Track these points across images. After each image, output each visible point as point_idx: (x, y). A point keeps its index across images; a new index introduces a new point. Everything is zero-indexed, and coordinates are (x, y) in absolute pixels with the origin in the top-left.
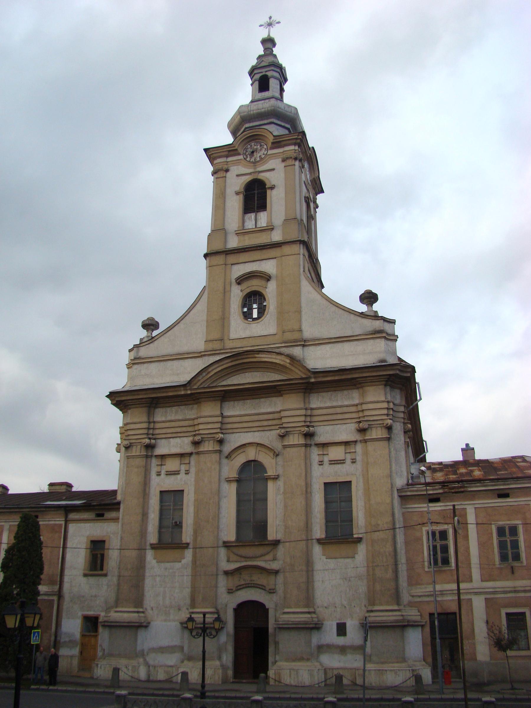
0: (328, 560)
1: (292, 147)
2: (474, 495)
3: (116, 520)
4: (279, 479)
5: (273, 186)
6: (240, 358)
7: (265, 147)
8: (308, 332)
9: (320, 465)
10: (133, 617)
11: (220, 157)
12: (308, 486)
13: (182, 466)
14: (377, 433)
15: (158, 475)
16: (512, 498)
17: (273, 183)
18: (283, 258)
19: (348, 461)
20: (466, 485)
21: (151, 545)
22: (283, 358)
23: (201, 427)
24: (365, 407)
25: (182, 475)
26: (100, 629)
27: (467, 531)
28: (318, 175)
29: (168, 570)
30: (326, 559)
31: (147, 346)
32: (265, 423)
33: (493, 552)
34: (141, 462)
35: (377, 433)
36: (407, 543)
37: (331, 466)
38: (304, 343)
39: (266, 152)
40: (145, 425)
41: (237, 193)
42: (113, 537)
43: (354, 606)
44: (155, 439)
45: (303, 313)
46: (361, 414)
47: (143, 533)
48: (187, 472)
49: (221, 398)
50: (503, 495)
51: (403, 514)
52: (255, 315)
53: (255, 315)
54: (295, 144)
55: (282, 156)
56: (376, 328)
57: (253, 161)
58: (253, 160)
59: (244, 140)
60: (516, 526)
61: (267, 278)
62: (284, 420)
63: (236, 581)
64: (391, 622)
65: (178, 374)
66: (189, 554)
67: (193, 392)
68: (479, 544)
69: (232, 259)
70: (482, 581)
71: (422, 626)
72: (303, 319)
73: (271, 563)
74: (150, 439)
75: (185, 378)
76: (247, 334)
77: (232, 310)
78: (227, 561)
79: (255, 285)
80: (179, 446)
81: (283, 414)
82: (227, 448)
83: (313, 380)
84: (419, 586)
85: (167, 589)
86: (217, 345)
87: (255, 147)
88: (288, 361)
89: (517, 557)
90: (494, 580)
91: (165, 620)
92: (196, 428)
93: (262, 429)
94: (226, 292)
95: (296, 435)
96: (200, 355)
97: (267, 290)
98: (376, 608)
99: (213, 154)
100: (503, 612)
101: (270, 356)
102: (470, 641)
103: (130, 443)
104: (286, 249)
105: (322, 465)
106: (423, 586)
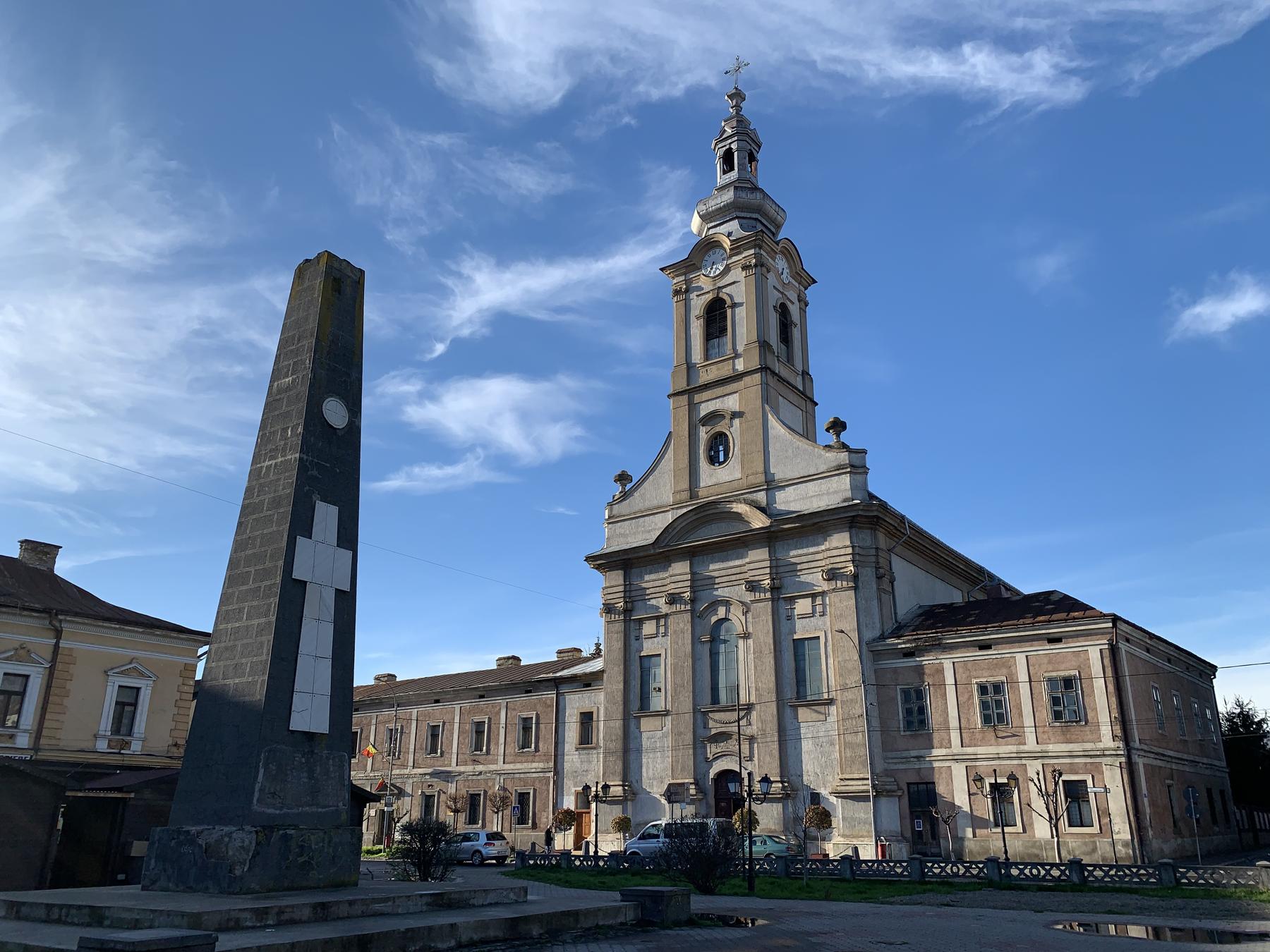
15: (636, 640)
32: (733, 578)
50: (985, 646)
51: (875, 671)
52: (722, 459)
53: (722, 459)
65: (649, 532)
85: (649, 760)
104: (747, 379)
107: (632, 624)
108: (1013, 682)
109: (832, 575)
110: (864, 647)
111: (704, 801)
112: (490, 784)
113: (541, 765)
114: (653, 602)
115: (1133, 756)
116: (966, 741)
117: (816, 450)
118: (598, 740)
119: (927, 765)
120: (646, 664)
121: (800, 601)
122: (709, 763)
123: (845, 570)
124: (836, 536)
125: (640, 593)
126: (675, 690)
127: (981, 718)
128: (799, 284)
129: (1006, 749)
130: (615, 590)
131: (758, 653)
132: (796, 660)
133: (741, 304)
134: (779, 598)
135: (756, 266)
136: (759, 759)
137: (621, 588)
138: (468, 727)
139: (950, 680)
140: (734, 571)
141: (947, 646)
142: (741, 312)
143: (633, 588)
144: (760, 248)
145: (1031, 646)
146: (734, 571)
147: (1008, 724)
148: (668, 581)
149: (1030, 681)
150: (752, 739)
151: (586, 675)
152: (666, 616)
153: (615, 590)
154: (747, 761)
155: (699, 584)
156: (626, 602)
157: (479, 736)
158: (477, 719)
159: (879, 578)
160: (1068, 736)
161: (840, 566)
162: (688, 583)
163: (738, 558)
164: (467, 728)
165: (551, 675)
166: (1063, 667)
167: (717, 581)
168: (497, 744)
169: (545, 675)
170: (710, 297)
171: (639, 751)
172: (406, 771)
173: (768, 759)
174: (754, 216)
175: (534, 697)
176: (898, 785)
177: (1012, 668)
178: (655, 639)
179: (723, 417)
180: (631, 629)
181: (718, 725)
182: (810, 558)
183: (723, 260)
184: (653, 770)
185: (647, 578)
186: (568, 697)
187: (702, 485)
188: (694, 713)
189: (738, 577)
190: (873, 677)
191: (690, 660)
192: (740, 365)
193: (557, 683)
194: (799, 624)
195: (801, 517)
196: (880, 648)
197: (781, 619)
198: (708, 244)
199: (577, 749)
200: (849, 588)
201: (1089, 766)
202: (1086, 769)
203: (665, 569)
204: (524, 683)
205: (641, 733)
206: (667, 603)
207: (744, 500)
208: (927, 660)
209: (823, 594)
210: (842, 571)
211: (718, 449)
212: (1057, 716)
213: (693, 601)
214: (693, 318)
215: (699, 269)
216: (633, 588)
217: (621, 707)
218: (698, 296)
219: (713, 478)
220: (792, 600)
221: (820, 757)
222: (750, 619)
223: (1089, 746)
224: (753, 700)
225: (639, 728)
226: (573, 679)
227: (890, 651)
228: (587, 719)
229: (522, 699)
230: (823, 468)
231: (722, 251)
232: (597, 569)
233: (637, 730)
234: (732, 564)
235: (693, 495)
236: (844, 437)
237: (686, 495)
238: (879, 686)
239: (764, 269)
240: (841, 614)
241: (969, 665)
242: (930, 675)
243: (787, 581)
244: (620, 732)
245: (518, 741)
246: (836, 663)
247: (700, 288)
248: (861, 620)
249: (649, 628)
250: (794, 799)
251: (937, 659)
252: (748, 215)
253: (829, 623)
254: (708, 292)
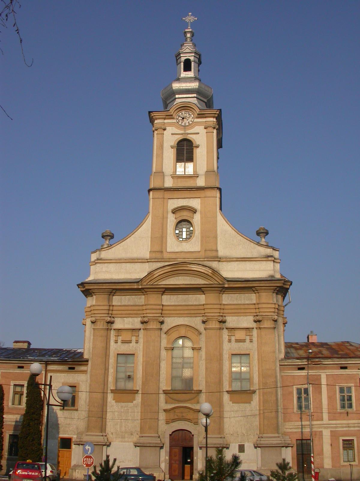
0: (233, 404)
1: (212, 119)
2: (325, 367)
3: (85, 372)
4: (201, 350)
5: (198, 146)
6: (177, 266)
7: (192, 116)
8: (221, 253)
10: (101, 439)
11: (159, 119)
12: (221, 355)
13: (133, 337)
14: (267, 324)
16: (349, 370)
17: (198, 143)
18: (206, 198)
19: (248, 340)
20: (322, 360)
21: (111, 390)
22: (207, 269)
23: (148, 311)
24: (260, 306)
25: (133, 344)
26: (73, 446)
27: (321, 389)
28: (221, 136)
29: (123, 408)
30: (232, 403)
31: (107, 251)
33: (337, 402)
34: (104, 333)
35: (267, 324)
36: (283, 395)
37: (236, 343)
38: (219, 260)
39: (193, 120)
40: (107, 308)
41: (172, 147)
42: (82, 384)
43: (250, 434)
44: (113, 318)
45: (219, 239)
46: (257, 311)
47: (105, 383)
48: (137, 342)
49: (162, 292)
52: (184, 236)
53: (184, 236)
54: (214, 117)
55: (205, 125)
56: (267, 254)
57: (184, 125)
58: (183, 124)
60: (350, 387)
61: (194, 211)
62: (206, 311)
63: (172, 416)
64: (274, 444)
66: (139, 398)
67: (143, 287)
68: (328, 398)
69: (167, 195)
70: (329, 420)
71: (292, 447)
72: (219, 244)
74: (110, 317)
77: (169, 232)
78: (166, 403)
79: (185, 215)
80: (131, 323)
81: (206, 307)
82: (165, 327)
83: (226, 286)
84: (290, 423)
86: (158, 255)
87: (185, 115)
88: (210, 272)
89: (350, 406)
90: (336, 420)
91: (122, 442)
92: (144, 312)
93: (190, 315)
94: (164, 218)
95: (214, 322)
96: (148, 261)
97: (194, 220)
98: (265, 435)
99: (154, 116)
100: (341, 438)
101: (198, 267)
102: (320, 456)
103: (96, 319)
104: (209, 193)
105: (230, 342)
106: (292, 423)
184: (125, 427)
221: (246, 424)
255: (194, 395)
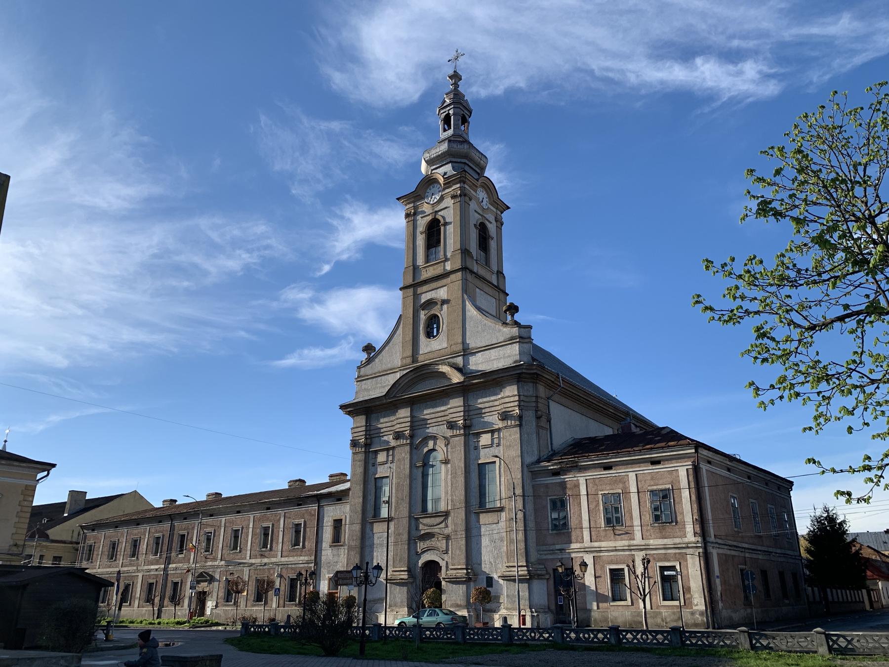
9: (475, 449)
32: (440, 419)
50: (608, 467)
51: (533, 486)
53: (435, 334)
59: (426, 183)
73: (443, 529)
75: (383, 392)
76: (429, 349)
104: (453, 277)
107: (370, 455)
108: (626, 492)
109: (505, 416)
110: (525, 469)
111: (415, 583)
112: (272, 572)
113: (306, 558)
114: (385, 438)
115: (708, 548)
116: (594, 537)
117: (497, 326)
118: (345, 540)
119: (567, 556)
120: (379, 484)
121: (483, 435)
122: (419, 555)
123: (513, 413)
124: (508, 388)
125: (376, 431)
126: (397, 503)
127: (604, 521)
128: (497, 209)
129: (621, 543)
130: (360, 429)
131: (454, 475)
132: (479, 479)
133: (450, 223)
134: (469, 434)
135: (460, 195)
136: (452, 552)
137: (364, 428)
138: (258, 531)
139: (583, 491)
140: (440, 414)
141: (581, 467)
142: (450, 229)
143: (372, 428)
144: (464, 183)
145: (640, 467)
146: (440, 414)
147: (622, 525)
148: (395, 422)
149: (638, 492)
150: (447, 538)
151: (337, 492)
152: (393, 448)
153: (360, 429)
154: (445, 554)
155: (417, 425)
156: (366, 439)
157: (266, 537)
158: (265, 525)
159: (538, 418)
160: (664, 533)
161: (510, 409)
162: (409, 424)
163: (443, 405)
164: (258, 531)
165: (315, 492)
166: (661, 482)
167: (429, 422)
168: (277, 543)
169: (311, 493)
170: (429, 218)
171: (372, 546)
172: (216, 563)
173: (458, 552)
174: (463, 161)
175: (303, 509)
176: (546, 571)
177: (626, 483)
178: (386, 465)
179: (436, 303)
180: (370, 458)
181: (426, 528)
182: (491, 404)
183: (439, 192)
185: (382, 420)
186: (326, 508)
187: (421, 352)
188: (410, 517)
189: (443, 419)
190: (531, 490)
191: (408, 480)
192: (448, 266)
193: (319, 498)
194: (483, 452)
195: (484, 374)
196: (536, 469)
197: (471, 449)
198: (428, 181)
199: (331, 546)
200: (515, 426)
201: (677, 555)
202: (676, 557)
203: (394, 413)
204: (297, 498)
205: (373, 534)
206: (394, 439)
207: (448, 363)
208: (569, 478)
209: (499, 430)
210: (511, 413)
211: (432, 326)
212: (657, 518)
213: (412, 437)
214: (418, 233)
215: (423, 198)
216: (372, 428)
217: (360, 516)
218: (422, 217)
219: (429, 347)
220: (478, 435)
222: (449, 450)
223: (677, 540)
224: (449, 508)
225: (372, 530)
226: (330, 495)
227: (543, 472)
228: (338, 524)
229: (295, 510)
230: (501, 339)
231: (439, 186)
232: (348, 414)
233: (371, 533)
234: (439, 409)
235: (414, 360)
236: (517, 317)
237: (409, 360)
238: (536, 496)
239: (467, 198)
240: (510, 446)
241: (597, 481)
242: (570, 489)
243: (475, 421)
244: (359, 534)
245: (291, 541)
246: (506, 480)
247: (423, 212)
248: (523, 449)
249: (381, 457)
250: (475, 581)
251: (575, 477)
252: (459, 160)
253: (502, 451)
254: (429, 215)
255: (442, 519)
